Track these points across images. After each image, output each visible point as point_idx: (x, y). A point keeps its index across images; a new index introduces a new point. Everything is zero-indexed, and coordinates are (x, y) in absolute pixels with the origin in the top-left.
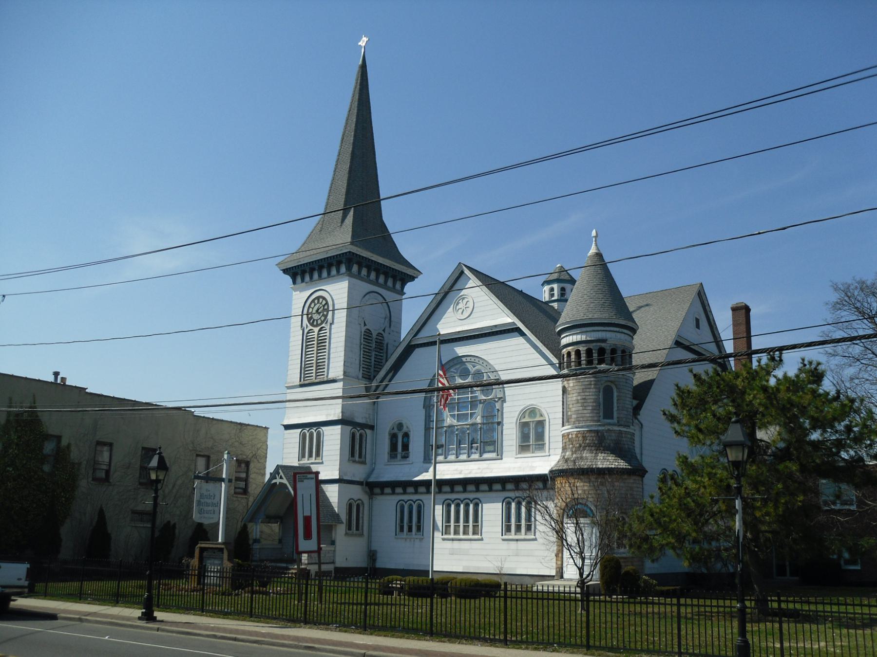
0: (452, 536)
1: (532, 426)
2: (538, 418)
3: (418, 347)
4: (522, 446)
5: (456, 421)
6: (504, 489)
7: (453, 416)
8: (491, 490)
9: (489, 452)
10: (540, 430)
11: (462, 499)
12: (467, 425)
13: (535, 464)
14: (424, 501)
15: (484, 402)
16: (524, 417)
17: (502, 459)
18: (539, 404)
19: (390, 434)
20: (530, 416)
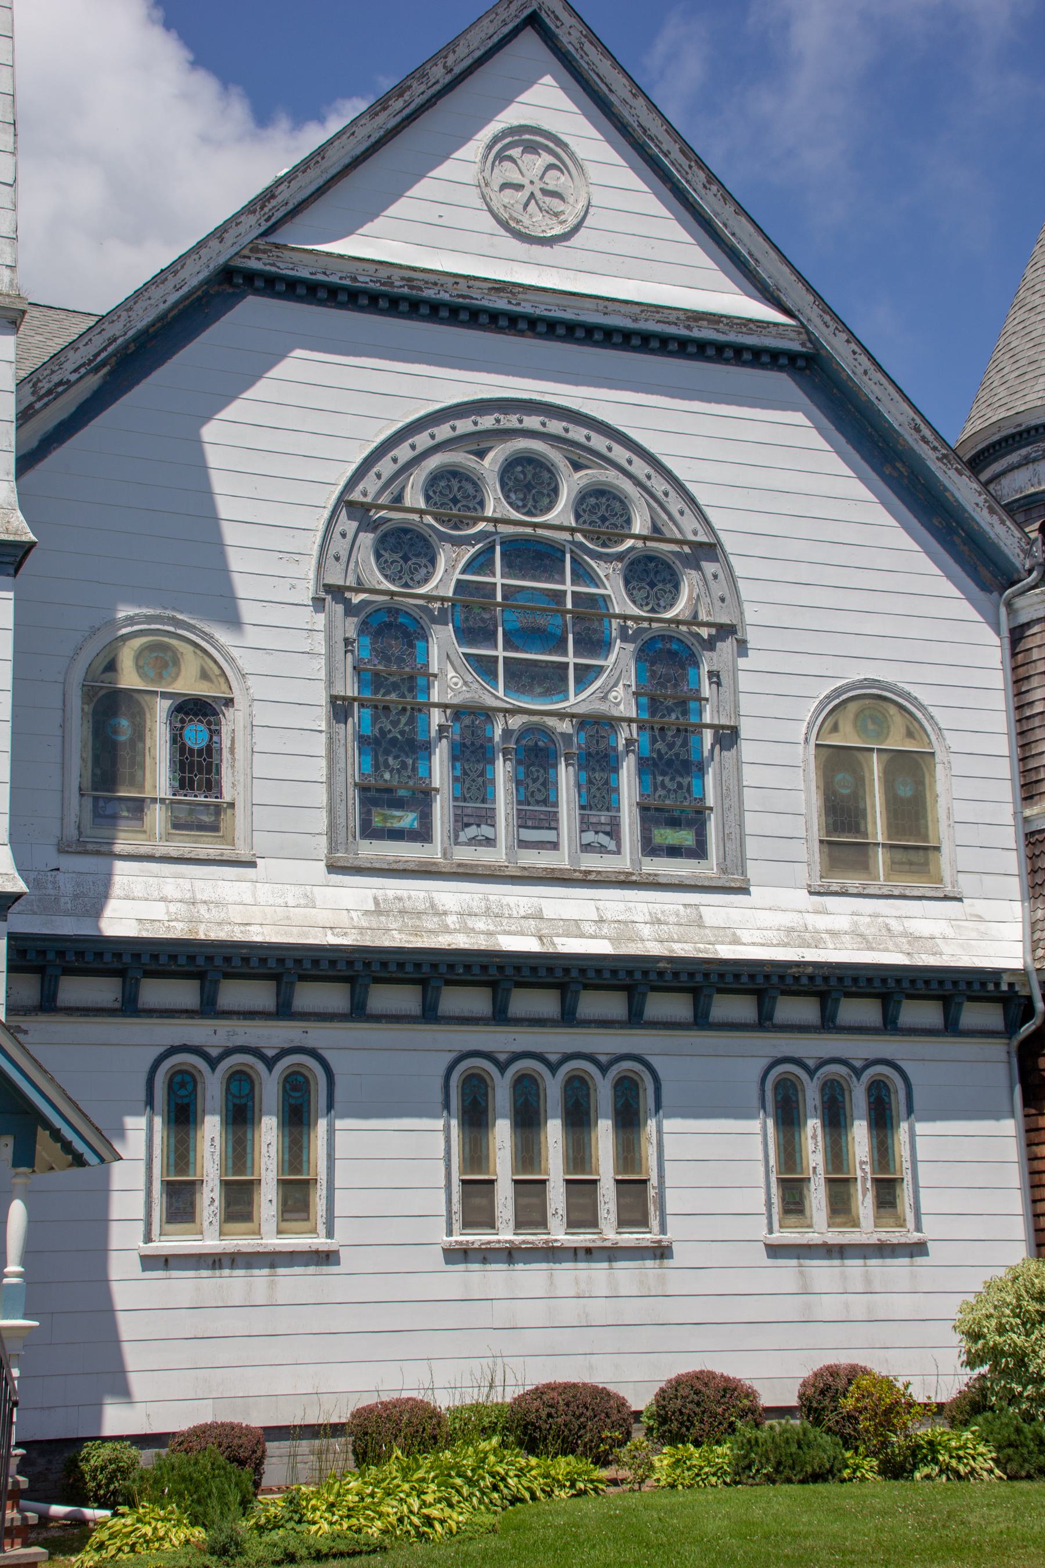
0: (506, 1235)
1: (876, 766)
2: (896, 742)
3: (257, 292)
4: (829, 843)
5: (501, 693)
6: (764, 1022)
7: (485, 667)
8: (701, 1021)
9: (674, 852)
10: (905, 791)
11: (858, 1064)
12: (561, 715)
13: (922, 927)
14: (655, 1061)
15: (639, 631)
16: (835, 728)
17: (744, 891)
18: (915, 691)
19: (89, 692)
20: (860, 724)
